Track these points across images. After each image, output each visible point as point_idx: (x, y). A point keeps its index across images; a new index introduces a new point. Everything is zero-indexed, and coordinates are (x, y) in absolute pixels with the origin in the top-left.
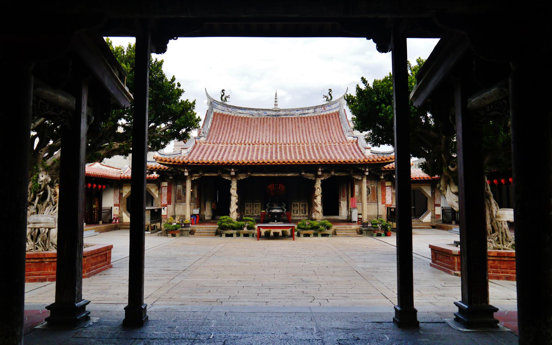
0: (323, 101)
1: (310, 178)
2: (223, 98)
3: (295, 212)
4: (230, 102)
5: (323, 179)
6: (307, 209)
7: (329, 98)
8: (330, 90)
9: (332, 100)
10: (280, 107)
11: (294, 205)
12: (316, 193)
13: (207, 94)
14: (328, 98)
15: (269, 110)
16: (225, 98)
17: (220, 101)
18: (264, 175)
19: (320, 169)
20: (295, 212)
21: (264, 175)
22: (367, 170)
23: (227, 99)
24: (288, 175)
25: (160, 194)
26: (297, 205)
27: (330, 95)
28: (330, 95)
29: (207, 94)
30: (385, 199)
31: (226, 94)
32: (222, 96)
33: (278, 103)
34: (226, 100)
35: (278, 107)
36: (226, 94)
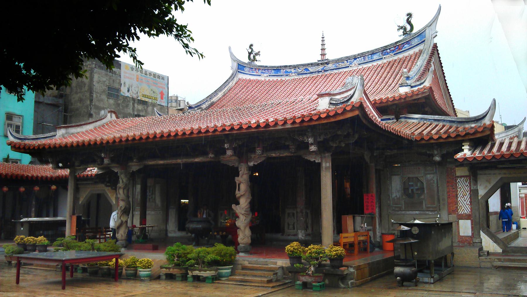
0: (397, 36)
1: (231, 165)
2: (252, 56)
3: (291, 227)
4: (262, 61)
5: (251, 164)
6: (310, 221)
7: (408, 28)
8: (410, 15)
9: (414, 31)
10: (330, 56)
11: (289, 214)
12: (237, 192)
13: (232, 54)
14: (405, 29)
15: (312, 64)
16: (254, 57)
17: (246, 60)
18: (161, 162)
19: (226, 146)
20: (291, 227)
21: (161, 162)
22: (311, 140)
23: (257, 57)
24: (197, 160)
25: (117, 199)
26: (293, 214)
27: (409, 22)
28: (409, 22)
29: (232, 54)
30: (456, 203)
31: (256, 50)
32: (250, 54)
33: (326, 51)
34: (255, 59)
35: (327, 57)
36: (256, 50)
